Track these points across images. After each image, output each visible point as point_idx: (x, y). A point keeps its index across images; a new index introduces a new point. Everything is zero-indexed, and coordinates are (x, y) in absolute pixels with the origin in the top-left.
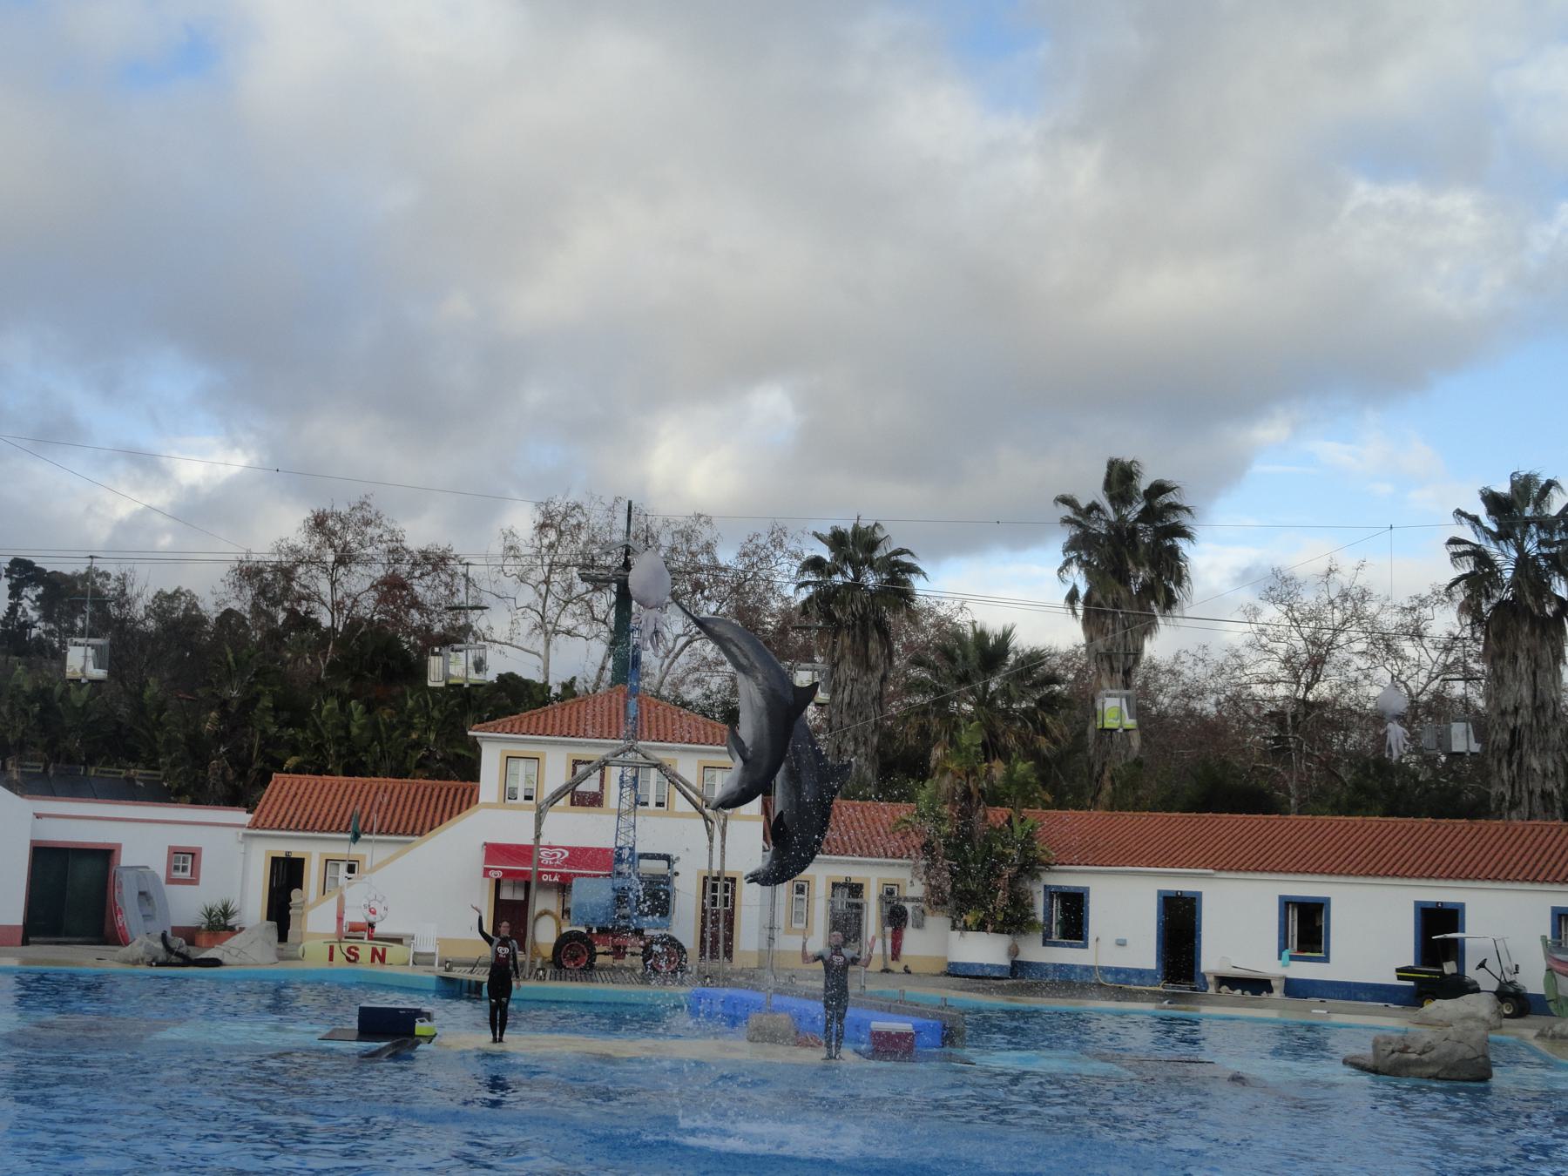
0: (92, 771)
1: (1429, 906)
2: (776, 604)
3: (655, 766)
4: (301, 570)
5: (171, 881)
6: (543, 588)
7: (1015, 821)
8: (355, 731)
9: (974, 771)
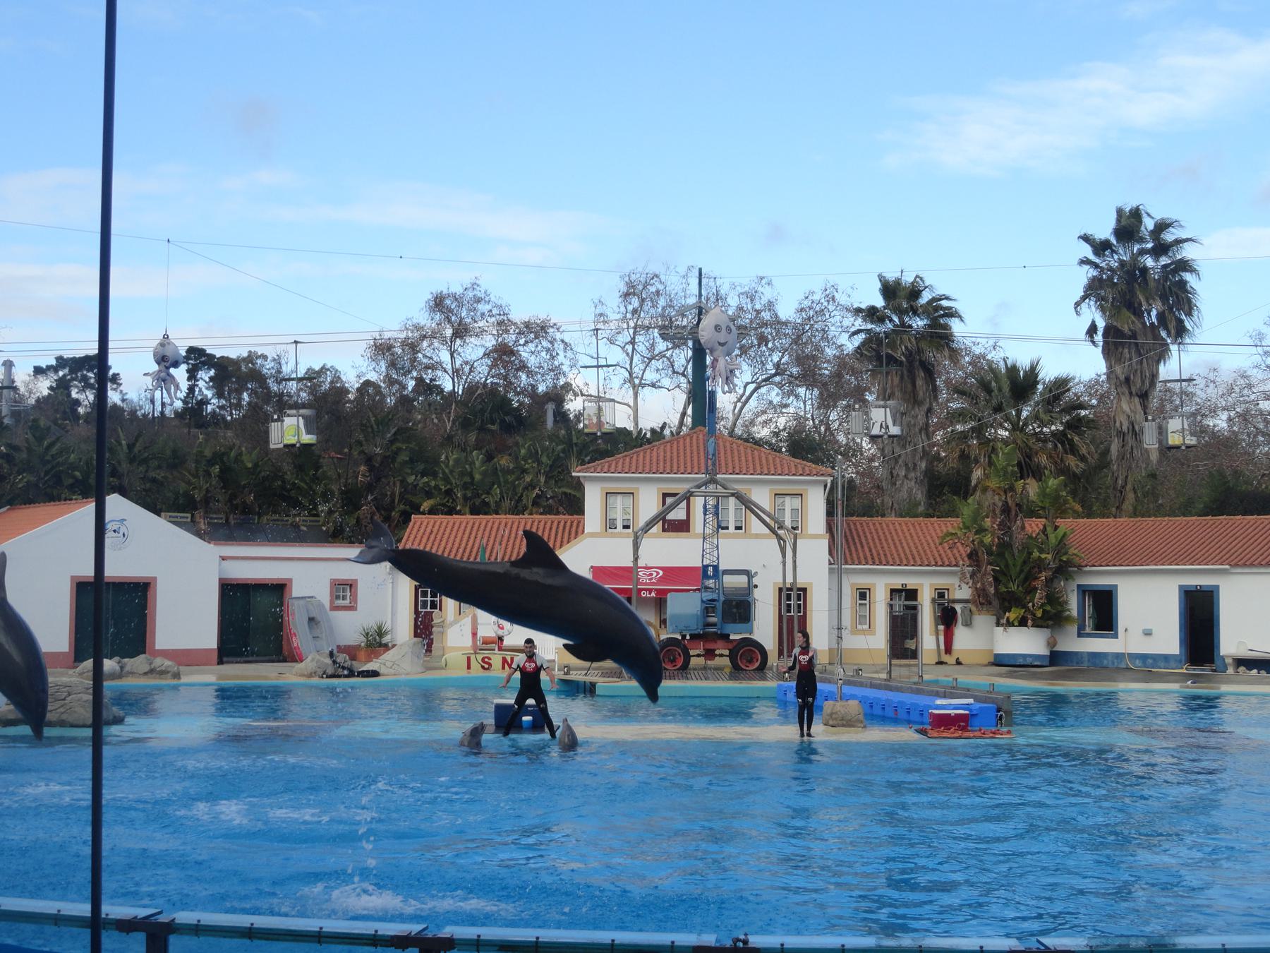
0: (264, 519)
2: (830, 352)
3: (733, 495)
4: (425, 344)
5: (335, 608)
6: (629, 348)
7: (1049, 529)
8: (477, 477)
9: (1012, 489)
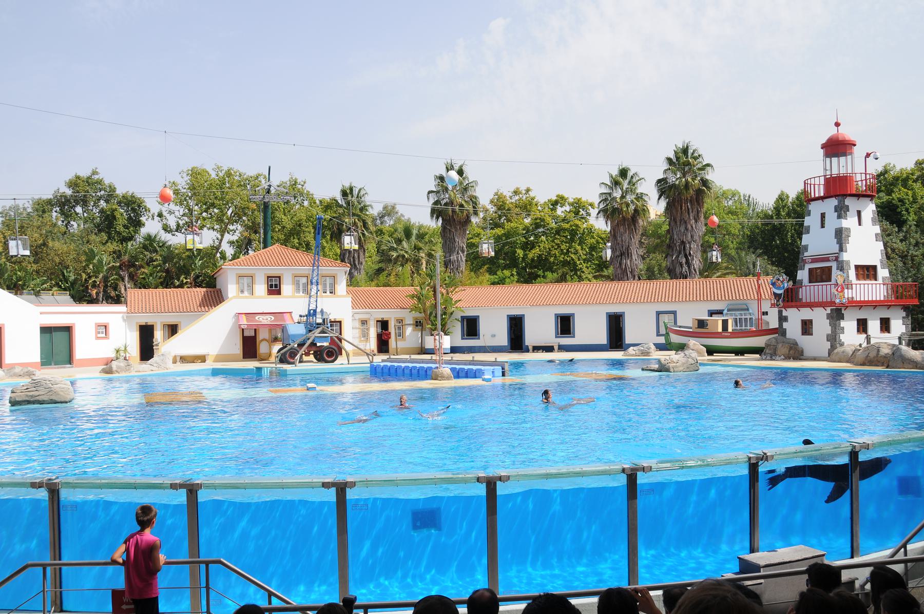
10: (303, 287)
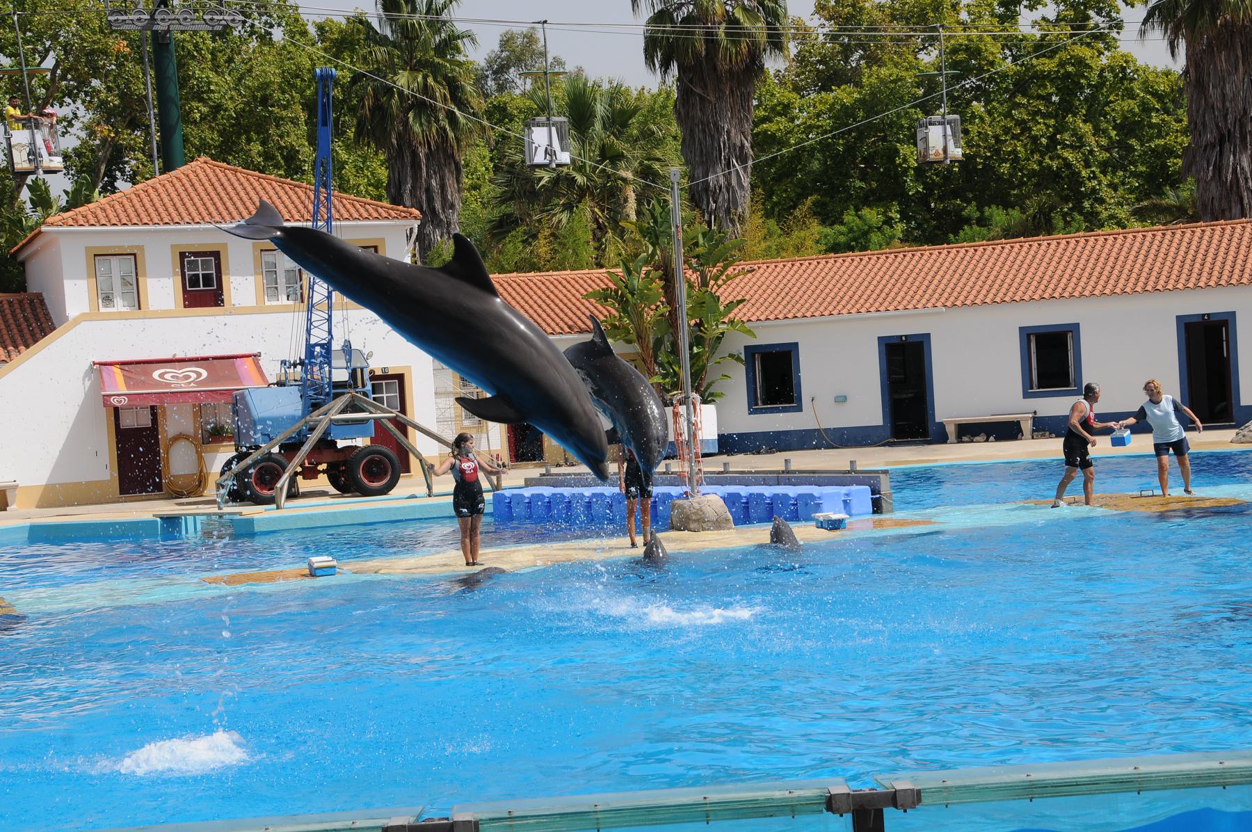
1: (1194, 320)
10: (288, 281)
